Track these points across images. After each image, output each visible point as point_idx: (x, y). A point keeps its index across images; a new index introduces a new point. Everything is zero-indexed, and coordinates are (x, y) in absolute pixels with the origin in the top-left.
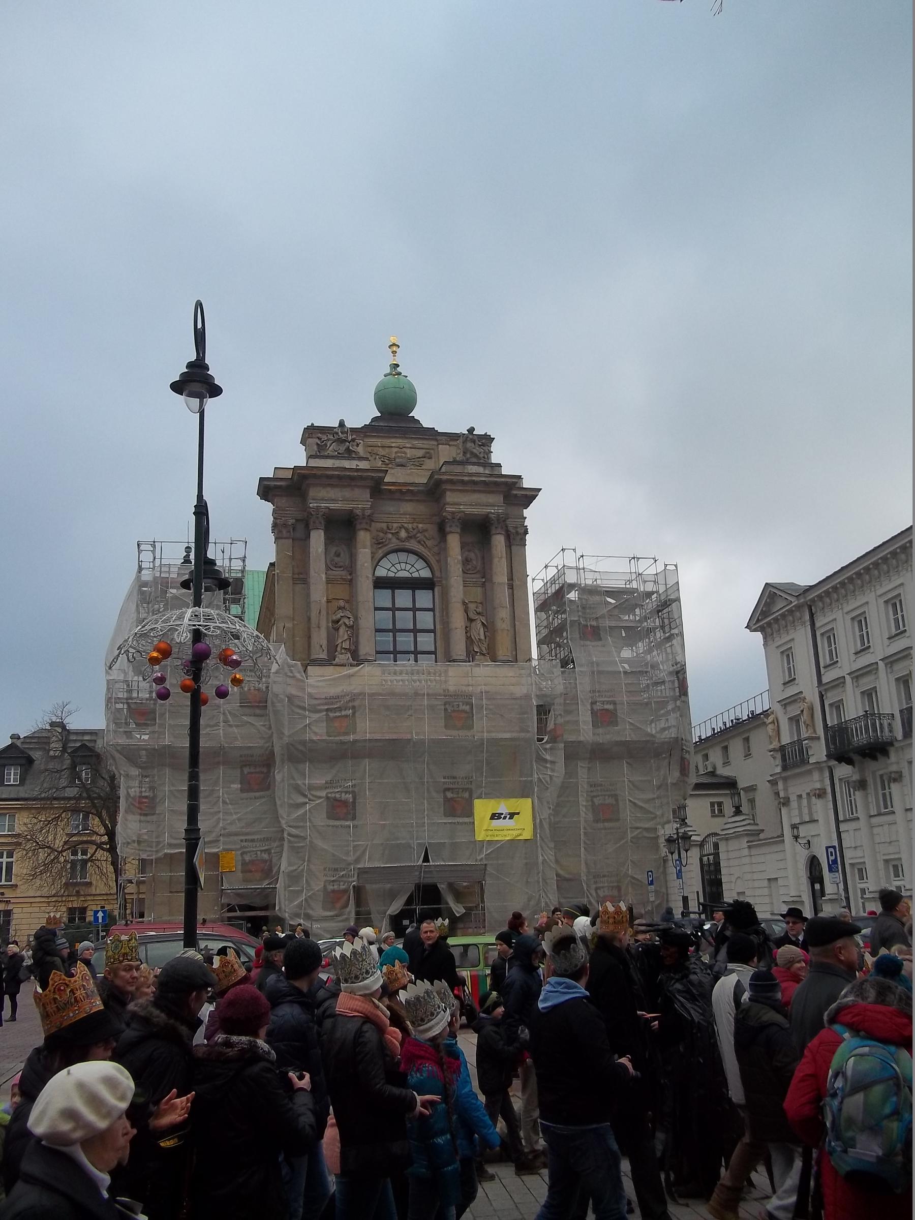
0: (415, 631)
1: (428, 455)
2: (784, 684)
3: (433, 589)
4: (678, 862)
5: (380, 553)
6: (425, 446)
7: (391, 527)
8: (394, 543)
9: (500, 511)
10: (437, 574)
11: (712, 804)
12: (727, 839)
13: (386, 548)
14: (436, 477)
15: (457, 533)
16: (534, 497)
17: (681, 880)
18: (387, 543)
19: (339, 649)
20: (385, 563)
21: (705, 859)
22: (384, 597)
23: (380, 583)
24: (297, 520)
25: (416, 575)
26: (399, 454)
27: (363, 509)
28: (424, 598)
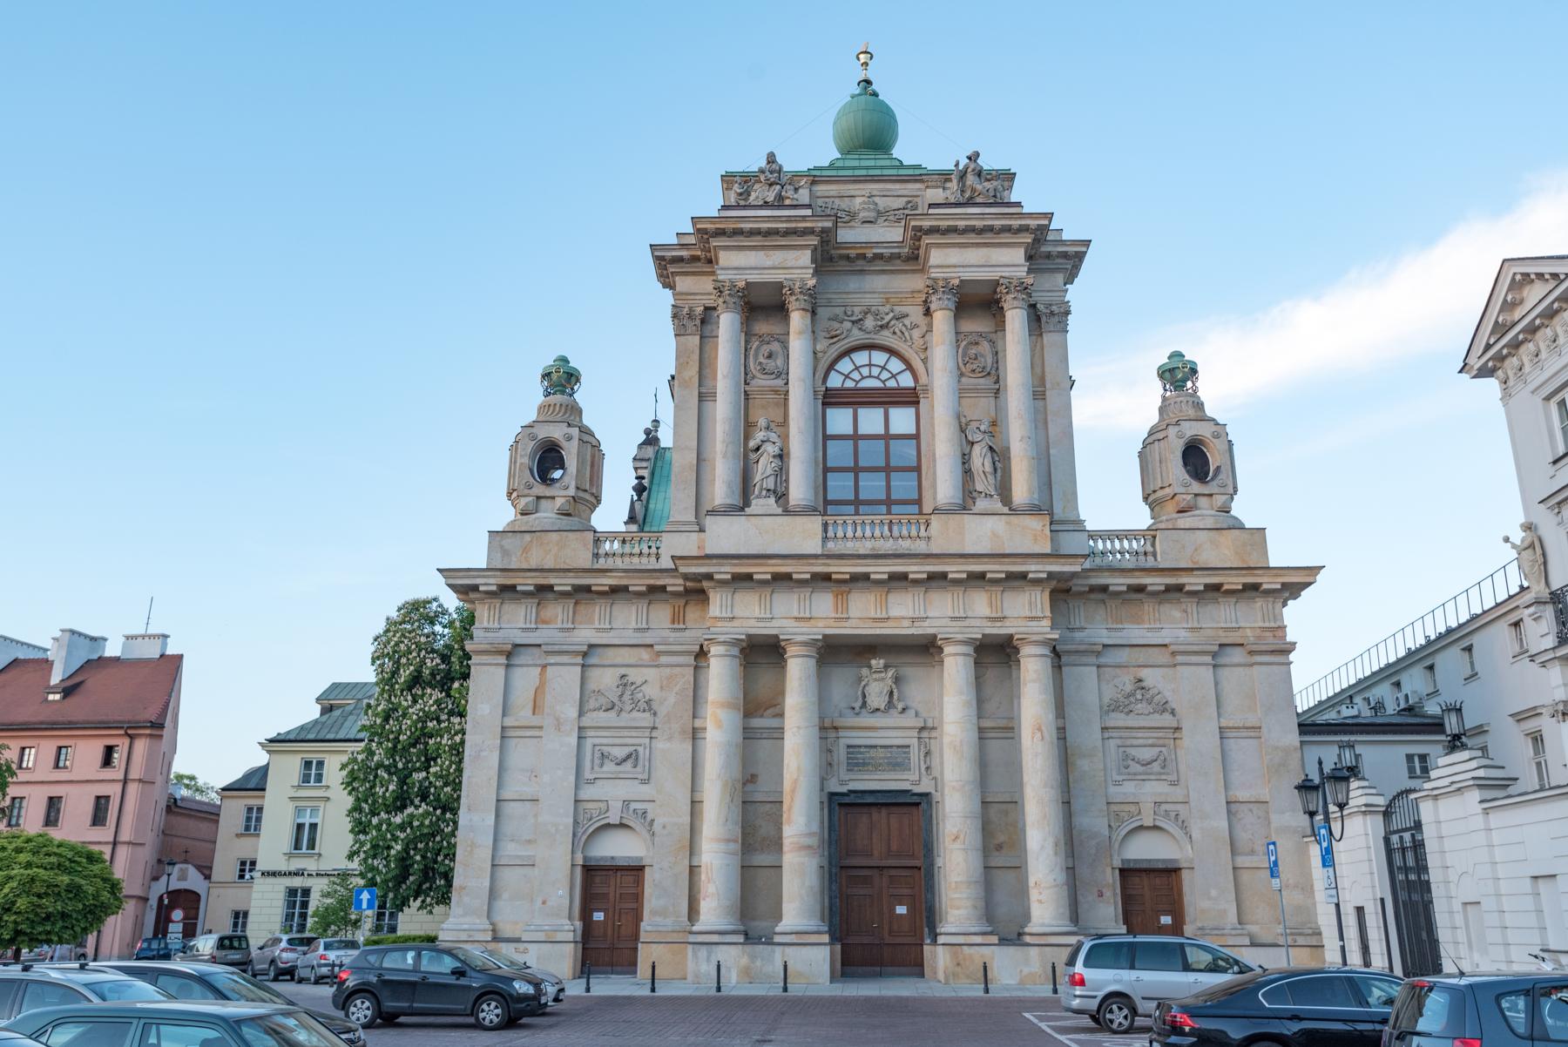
0: (887, 469)
1: (909, 206)
2: (1555, 462)
3: (915, 403)
4: (1323, 831)
5: (833, 352)
6: (905, 193)
7: (849, 313)
8: (857, 336)
9: (1018, 274)
10: (923, 379)
11: (1410, 758)
12: (1436, 797)
13: (843, 343)
14: (913, 223)
15: (951, 310)
16: (1080, 257)
17: (1331, 870)
18: (843, 337)
19: (756, 492)
20: (845, 366)
21: (1395, 838)
22: (840, 421)
23: (831, 399)
24: (707, 309)
25: (892, 384)
26: (866, 206)
27: (802, 280)
28: (902, 420)
